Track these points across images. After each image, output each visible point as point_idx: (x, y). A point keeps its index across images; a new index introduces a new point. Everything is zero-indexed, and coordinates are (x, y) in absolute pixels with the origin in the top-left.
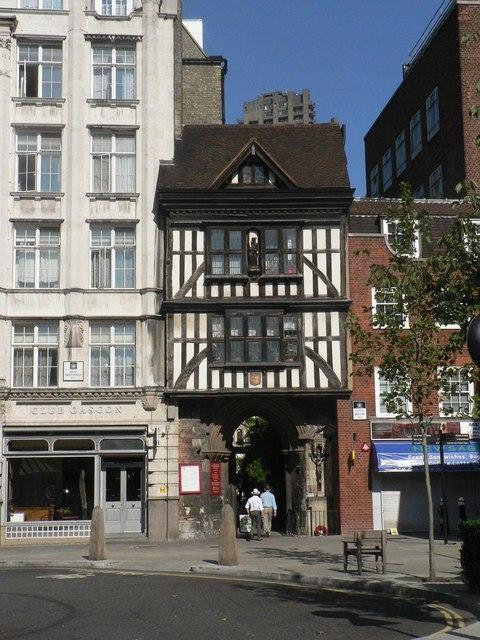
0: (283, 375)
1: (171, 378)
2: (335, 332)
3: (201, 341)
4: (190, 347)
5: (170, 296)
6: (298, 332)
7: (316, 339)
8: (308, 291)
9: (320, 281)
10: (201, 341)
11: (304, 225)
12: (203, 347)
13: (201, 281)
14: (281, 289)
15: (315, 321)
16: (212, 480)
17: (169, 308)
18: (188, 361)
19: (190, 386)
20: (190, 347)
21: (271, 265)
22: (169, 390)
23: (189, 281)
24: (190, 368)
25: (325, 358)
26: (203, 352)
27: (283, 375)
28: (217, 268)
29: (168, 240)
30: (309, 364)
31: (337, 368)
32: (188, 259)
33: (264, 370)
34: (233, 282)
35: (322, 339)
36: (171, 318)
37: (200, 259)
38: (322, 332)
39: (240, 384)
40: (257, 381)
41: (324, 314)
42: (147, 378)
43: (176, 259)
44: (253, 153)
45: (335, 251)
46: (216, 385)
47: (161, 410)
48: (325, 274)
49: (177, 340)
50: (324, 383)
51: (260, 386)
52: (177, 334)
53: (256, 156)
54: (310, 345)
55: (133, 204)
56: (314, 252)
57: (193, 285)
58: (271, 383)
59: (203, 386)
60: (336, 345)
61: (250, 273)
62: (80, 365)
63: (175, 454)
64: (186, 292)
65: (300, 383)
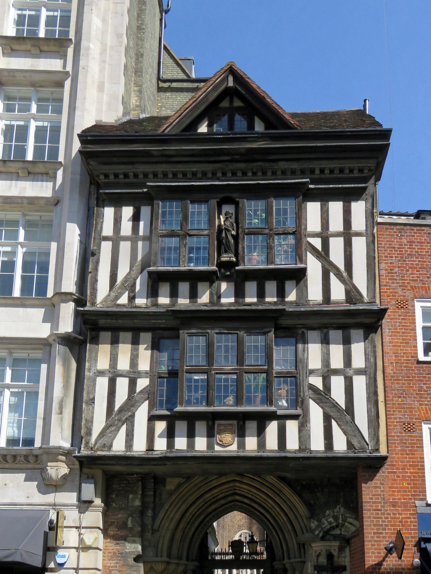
3: (140, 375)
18: (117, 406)
22: (84, 452)
23: (126, 279)
25: (342, 402)
26: (141, 392)
35: (336, 372)
41: (340, 332)
45: (358, 234)
48: (342, 267)
61: (221, 265)
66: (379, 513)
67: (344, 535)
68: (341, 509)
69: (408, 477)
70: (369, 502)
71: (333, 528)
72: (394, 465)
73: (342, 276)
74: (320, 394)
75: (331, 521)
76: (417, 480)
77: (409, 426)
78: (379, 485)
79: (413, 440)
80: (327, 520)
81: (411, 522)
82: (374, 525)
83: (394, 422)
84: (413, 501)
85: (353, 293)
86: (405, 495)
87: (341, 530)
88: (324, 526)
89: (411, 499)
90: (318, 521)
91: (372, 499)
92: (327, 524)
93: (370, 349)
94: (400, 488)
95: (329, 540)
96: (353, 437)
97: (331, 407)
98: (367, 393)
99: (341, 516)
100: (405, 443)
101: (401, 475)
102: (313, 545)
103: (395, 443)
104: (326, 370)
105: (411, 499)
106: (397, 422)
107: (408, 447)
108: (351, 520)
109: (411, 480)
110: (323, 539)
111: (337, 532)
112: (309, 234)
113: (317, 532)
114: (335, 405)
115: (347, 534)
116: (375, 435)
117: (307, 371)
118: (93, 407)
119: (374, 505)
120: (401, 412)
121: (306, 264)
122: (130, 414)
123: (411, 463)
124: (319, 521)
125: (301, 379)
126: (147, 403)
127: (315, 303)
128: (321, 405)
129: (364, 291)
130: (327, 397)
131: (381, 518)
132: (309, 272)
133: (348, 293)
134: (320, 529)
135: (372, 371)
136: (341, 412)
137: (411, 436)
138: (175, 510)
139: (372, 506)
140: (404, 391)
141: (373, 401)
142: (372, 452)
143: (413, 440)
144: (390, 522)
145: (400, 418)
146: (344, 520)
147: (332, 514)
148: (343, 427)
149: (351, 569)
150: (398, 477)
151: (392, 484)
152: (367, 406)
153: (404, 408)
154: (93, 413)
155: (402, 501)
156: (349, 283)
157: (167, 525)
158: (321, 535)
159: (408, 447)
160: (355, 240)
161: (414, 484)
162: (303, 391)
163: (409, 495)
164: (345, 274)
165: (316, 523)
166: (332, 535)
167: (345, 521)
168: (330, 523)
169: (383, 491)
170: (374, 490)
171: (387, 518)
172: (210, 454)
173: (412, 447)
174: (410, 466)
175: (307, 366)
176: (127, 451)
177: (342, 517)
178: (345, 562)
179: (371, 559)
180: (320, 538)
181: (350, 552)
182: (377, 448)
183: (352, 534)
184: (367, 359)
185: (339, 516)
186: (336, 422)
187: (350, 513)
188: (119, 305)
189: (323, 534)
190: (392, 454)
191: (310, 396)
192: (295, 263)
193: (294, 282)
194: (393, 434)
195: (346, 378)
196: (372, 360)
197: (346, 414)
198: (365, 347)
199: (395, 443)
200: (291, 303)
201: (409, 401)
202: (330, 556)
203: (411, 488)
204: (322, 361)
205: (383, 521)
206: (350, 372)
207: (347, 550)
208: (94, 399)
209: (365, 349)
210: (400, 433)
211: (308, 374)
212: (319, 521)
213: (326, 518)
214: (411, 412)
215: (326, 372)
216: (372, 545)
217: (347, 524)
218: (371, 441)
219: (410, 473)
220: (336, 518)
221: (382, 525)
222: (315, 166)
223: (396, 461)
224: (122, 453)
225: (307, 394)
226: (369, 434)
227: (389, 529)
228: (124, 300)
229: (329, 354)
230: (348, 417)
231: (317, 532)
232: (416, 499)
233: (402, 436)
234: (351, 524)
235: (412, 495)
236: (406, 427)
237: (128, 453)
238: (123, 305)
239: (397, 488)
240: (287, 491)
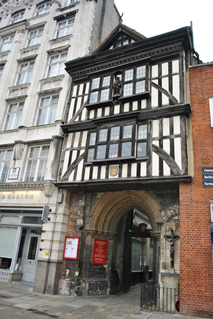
0: (134, 166)
1: (60, 174)
2: (177, 131)
4: (75, 153)
5: (66, 123)
6: (149, 135)
7: (161, 138)
8: (154, 103)
9: (164, 97)
10: (81, 148)
11: (152, 63)
12: (82, 152)
13: (85, 111)
14: (135, 105)
15: (161, 125)
17: (67, 129)
19: (71, 179)
20: (75, 153)
21: (128, 91)
23: (78, 112)
24: (73, 166)
26: (81, 156)
27: (134, 166)
28: (94, 100)
29: (72, 90)
30: (155, 158)
31: (178, 159)
32: (80, 99)
33: (120, 162)
34: (103, 105)
35: (166, 137)
36: (67, 136)
37: (86, 98)
38: (166, 133)
39: (103, 177)
40: (114, 173)
41: (168, 119)
42: (48, 177)
43: (73, 101)
45: (175, 74)
46: (87, 178)
47: (56, 196)
49: (67, 149)
50: (167, 172)
51: (117, 177)
52: (69, 145)
53: (122, 32)
54: (156, 143)
55: (61, 82)
56: (160, 79)
57: (80, 114)
58: (124, 175)
59: (79, 179)
60: (178, 142)
61: (114, 98)
62: (18, 169)
63: (59, 228)
64: (75, 119)
65: (148, 172)
66: (188, 207)
70: (183, 201)
71: (173, 216)
73: (168, 94)
74: (158, 149)
77: (206, 160)
78: (189, 192)
81: (207, 211)
82: (186, 213)
85: (173, 100)
91: (185, 199)
93: (183, 125)
97: (164, 154)
104: (161, 137)
106: (199, 159)
114: (165, 154)
118: (63, 164)
119: (186, 202)
120: (202, 154)
122: (76, 165)
125: (149, 143)
126: (83, 160)
127: (155, 107)
128: (158, 153)
129: (178, 98)
130: (161, 149)
131: (190, 209)
133: (170, 100)
135: (184, 134)
136: (168, 156)
138: (99, 207)
139: (185, 203)
140: (204, 143)
144: (195, 211)
145: (201, 157)
153: (203, 152)
154: (63, 166)
156: (171, 96)
157: (95, 214)
160: (173, 77)
162: (150, 148)
164: (169, 93)
169: (191, 195)
170: (186, 195)
172: (107, 180)
175: (152, 136)
176: (74, 181)
179: (183, 231)
182: (186, 173)
184: (181, 129)
186: (165, 161)
188: (75, 122)
191: (153, 150)
194: (197, 165)
196: (184, 130)
197: (170, 157)
198: (180, 124)
199: (198, 170)
200: (144, 109)
201: (206, 148)
204: (159, 133)
205: (190, 211)
206: (172, 137)
208: (64, 160)
209: (181, 125)
214: (207, 153)
215: (161, 138)
216: (184, 224)
220: (175, 211)
221: (190, 213)
224: (72, 182)
225: (151, 149)
227: (194, 215)
229: (163, 130)
230: (172, 158)
236: (205, 161)
237: (75, 182)
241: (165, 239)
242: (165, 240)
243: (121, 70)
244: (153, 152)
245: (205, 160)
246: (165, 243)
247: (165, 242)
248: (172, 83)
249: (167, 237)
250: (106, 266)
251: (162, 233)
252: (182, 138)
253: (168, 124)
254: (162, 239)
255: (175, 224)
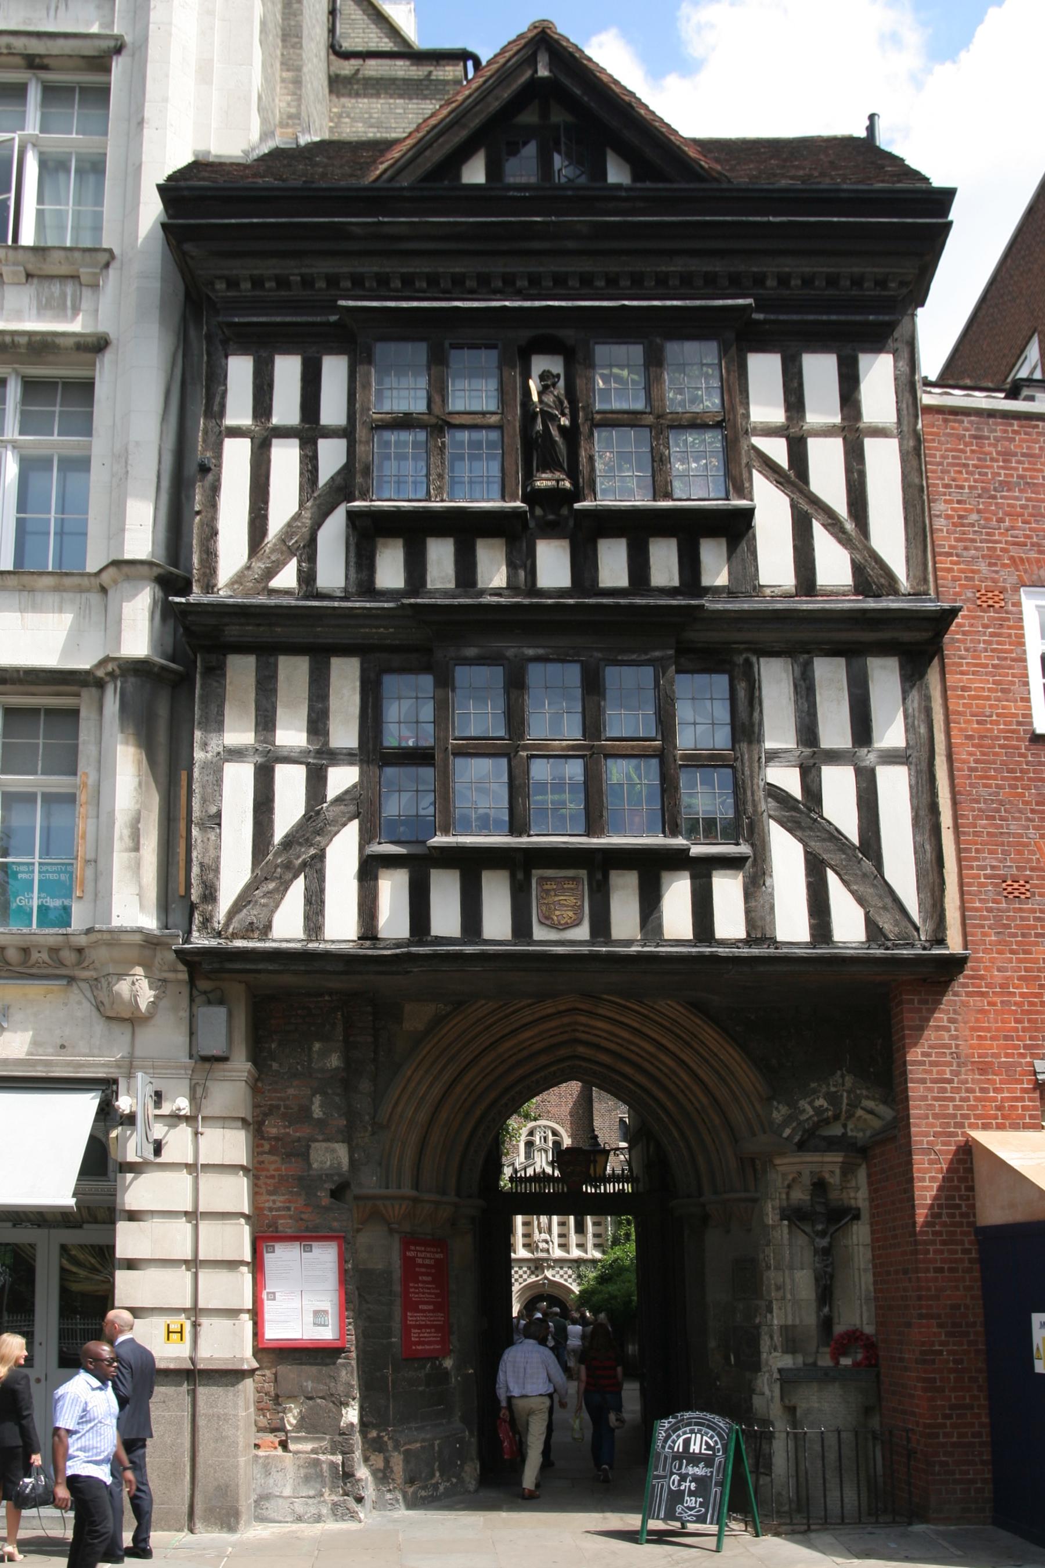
16: (410, 1305)
35: (834, 757)
44: (543, 72)
48: (838, 501)
67: (852, 1137)
68: (847, 1078)
69: (1016, 1004)
72: (982, 978)
75: (822, 1106)
76: (1037, 1012)
79: (1027, 919)
80: (811, 1103)
83: (978, 877)
84: (1028, 1059)
86: (1007, 1047)
87: (845, 1126)
88: (803, 1117)
89: (1023, 1056)
90: (788, 1105)
92: (811, 1112)
94: (998, 1030)
95: (816, 1150)
96: (881, 912)
98: (912, 808)
99: (845, 1094)
100: (1008, 926)
101: (998, 1000)
102: (777, 1161)
103: (983, 927)
105: (1023, 1056)
106: (986, 877)
107: (1015, 935)
108: (870, 1104)
109: (1023, 1012)
110: (801, 1146)
111: (836, 1130)
112: (755, 428)
113: (787, 1132)
115: (860, 1135)
116: (934, 905)
117: (760, 752)
121: (752, 500)
123: (1023, 973)
124: (792, 1104)
132: (760, 520)
134: (794, 1124)
137: (1021, 910)
141: (928, 827)
142: (927, 945)
143: (1027, 919)
146: (854, 1105)
147: (824, 1089)
148: (855, 887)
149: (872, 1216)
150: (990, 1004)
151: (977, 1020)
152: (914, 838)
155: (1003, 1059)
158: (797, 1139)
159: (1015, 935)
161: (1029, 1021)
162: (754, 800)
163: (1018, 1047)
165: (784, 1110)
166: (825, 1138)
167: (856, 1107)
168: (819, 1111)
171: (962, 1099)
173: (1023, 935)
174: (1020, 978)
177: (848, 1097)
178: (856, 1199)
180: (796, 1144)
181: (869, 1176)
183: (870, 1137)
185: (842, 1096)
187: (867, 1088)
189: (802, 1136)
190: (976, 951)
192: (723, 495)
193: (723, 542)
194: (978, 905)
195: (859, 772)
197: (860, 856)
199: (983, 927)
202: (820, 1186)
203: (1024, 1030)
207: (862, 1174)
210: (994, 901)
211: (763, 760)
212: (792, 1104)
213: (808, 1100)
217: (860, 1112)
218: (924, 921)
219: (1022, 995)
222: (765, 269)
223: (986, 969)
226: (920, 905)
228: (287, 578)
230: (868, 865)
231: (787, 1132)
232: (1034, 1056)
233: (999, 910)
234: (871, 1112)
235: (1026, 1047)
238: (287, 592)
239: (988, 1030)
240: (709, 1035)
241: (786, 1222)
242: (786, 1231)
243: (568, 334)
244: (771, 822)
245: (1022, 882)
246: (786, 1242)
247: (786, 1236)
248: (848, 471)
249: (795, 1216)
250: (448, 1363)
251: (773, 1199)
252: (913, 767)
253: (841, 689)
254: (774, 1227)
255: (840, 1159)
